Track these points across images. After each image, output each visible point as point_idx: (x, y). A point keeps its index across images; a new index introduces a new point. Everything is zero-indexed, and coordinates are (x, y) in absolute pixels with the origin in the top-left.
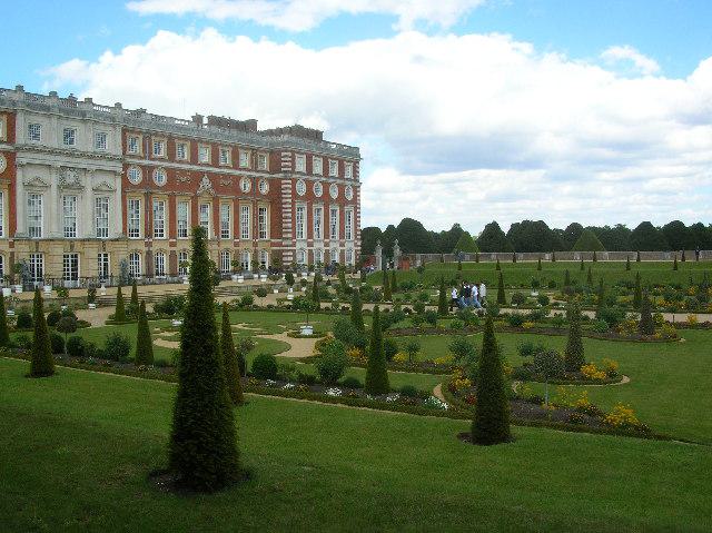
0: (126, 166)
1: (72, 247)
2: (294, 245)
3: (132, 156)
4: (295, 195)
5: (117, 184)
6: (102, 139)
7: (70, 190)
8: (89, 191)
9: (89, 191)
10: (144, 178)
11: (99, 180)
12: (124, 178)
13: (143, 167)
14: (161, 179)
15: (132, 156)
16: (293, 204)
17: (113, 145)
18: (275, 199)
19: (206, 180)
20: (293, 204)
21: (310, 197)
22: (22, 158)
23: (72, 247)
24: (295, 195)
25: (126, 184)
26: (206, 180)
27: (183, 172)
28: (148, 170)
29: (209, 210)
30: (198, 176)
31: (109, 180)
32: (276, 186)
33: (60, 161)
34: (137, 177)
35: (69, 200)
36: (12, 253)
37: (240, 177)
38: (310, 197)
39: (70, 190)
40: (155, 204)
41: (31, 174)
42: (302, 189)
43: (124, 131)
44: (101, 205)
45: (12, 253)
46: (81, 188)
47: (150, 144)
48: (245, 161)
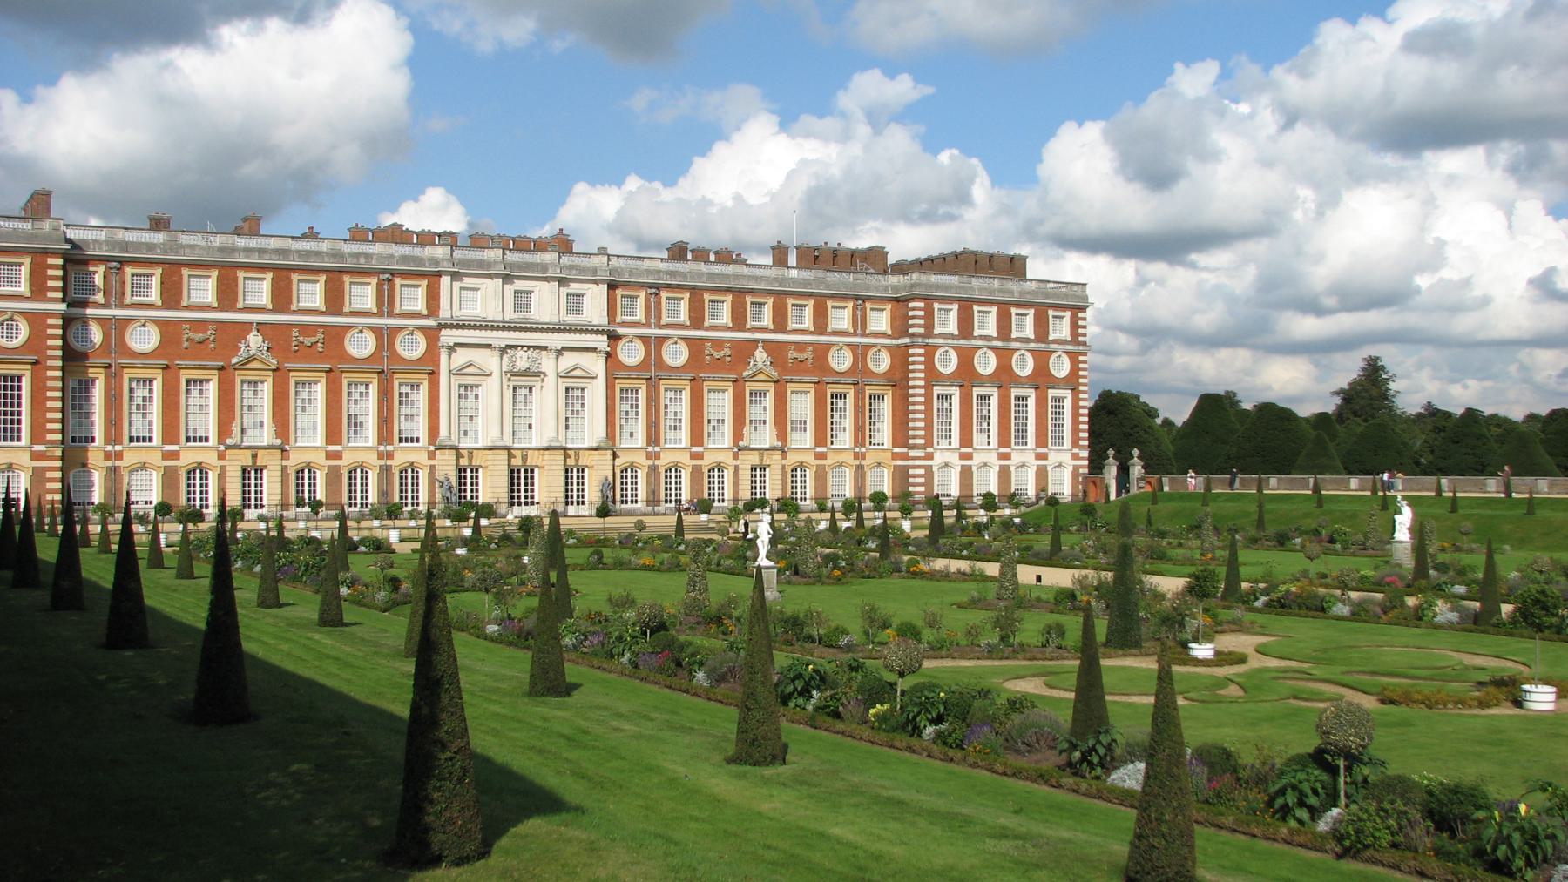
0: (614, 338)
1: (524, 458)
2: (930, 457)
3: (624, 324)
4: (933, 377)
5: (597, 365)
7: (523, 381)
8: (551, 379)
9: (551, 379)
11: (569, 360)
12: (609, 356)
13: (645, 339)
14: (676, 355)
15: (624, 324)
16: (929, 387)
18: (898, 380)
19: (760, 356)
21: (966, 376)
22: (448, 337)
23: (524, 458)
24: (933, 377)
26: (760, 356)
27: (718, 343)
28: (654, 345)
29: (769, 401)
30: (744, 351)
32: (900, 356)
33: (501, 338)
34: (632, 354)
36: (433, 467)
38: (966, 376)
39: (523, 381)
40: (665, 396)
41: (461, 357)
42: (948, 363)
43: (612, 286)
44: (572, 395)
45: (433, 467)
46: (539, 374)
47: (658, 304)
48: (841, 318)
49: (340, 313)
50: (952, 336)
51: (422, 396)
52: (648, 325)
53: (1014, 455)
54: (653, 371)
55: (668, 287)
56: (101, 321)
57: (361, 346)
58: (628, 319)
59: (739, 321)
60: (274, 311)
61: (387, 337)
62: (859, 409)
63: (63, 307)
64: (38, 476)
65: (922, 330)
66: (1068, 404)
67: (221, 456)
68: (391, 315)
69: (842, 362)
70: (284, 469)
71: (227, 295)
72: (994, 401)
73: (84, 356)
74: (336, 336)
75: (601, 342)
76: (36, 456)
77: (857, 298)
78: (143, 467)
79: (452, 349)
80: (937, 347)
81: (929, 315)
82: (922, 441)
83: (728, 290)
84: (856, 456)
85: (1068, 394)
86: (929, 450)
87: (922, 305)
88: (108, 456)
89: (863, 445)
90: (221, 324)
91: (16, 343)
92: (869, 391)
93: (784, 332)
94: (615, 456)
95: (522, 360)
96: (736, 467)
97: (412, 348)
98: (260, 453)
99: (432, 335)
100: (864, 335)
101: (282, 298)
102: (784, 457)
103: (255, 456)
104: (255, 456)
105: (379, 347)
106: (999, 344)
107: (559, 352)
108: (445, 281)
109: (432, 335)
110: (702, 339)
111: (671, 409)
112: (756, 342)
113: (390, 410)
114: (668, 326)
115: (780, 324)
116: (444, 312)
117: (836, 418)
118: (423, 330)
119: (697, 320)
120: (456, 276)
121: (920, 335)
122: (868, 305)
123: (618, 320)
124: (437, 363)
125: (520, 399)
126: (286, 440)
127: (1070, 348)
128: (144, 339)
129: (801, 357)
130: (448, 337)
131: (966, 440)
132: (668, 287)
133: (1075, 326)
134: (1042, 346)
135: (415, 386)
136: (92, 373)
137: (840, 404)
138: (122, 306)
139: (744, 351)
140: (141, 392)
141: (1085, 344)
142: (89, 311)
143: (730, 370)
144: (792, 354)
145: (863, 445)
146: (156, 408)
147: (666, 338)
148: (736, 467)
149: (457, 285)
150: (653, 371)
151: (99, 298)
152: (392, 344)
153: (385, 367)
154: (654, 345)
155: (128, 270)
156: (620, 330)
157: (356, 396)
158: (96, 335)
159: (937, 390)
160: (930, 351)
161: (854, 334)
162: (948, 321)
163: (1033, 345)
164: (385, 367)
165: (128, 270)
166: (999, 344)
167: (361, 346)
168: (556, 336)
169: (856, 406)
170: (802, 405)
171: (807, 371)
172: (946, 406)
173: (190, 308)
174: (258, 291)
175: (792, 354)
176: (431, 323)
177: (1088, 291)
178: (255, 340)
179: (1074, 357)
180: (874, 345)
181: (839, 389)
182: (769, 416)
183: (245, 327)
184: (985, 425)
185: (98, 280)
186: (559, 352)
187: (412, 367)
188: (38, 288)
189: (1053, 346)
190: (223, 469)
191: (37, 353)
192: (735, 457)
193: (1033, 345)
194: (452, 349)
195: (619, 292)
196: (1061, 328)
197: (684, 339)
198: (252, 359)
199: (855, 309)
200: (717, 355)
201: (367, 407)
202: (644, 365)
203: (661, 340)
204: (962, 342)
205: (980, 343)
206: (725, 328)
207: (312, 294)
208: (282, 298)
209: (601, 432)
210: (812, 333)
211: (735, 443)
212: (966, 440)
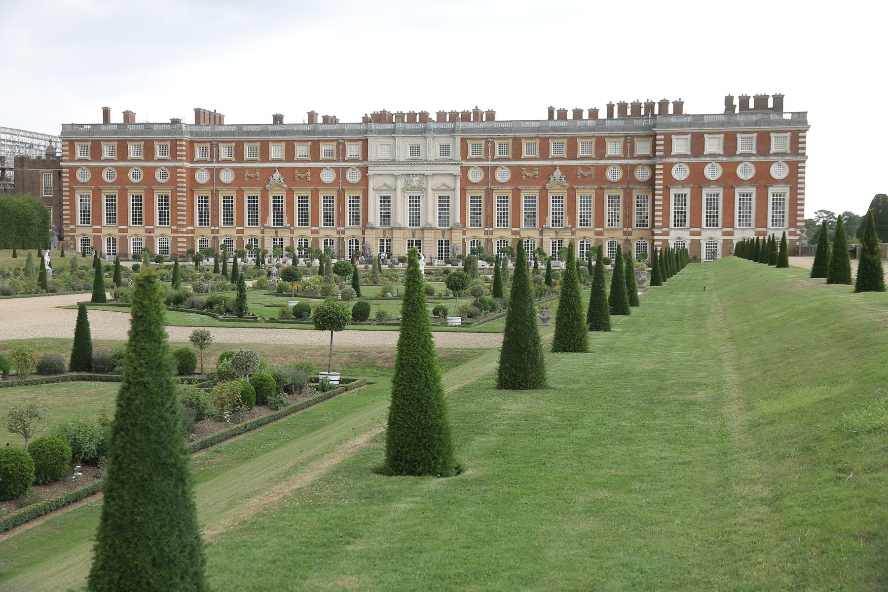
0: (465, 170)
3: (472, 160)
9: (430, 191)
10: (486, 176)
13: (485, 168)
14: (503, 176)
15: (472, 160)
16: (667, 189)
17: (456, 152)
19: (558, 174)
20: (667, 189)
22: (370, 172)
24: (670, 182)
25: (466, 183)
26: (558, 174)
27: (531, 168)
28: (489, 172)
31: (449, 181)
34: (475, 176)
37: (606, 167)
47: (493, 147)
49: (318, 161)
50: (686, 156)
52: (487, 160)
53: (736, 232)
57: (327, 177)
58: (474, 156)
60: (287, 161)
65: (662, 153)
66: (787, 197)
67: (263, 232)
68: (344, 161)
71: (265, 154)
74: (317, 172)
75: (457, 170)
76: (174, 231)
80: (672, 165)
82: (661, 224)
83: (536, 138)
84: (625, 233)
85: (785, 190)
88: (213, 232)
89: (630, 226)
90: (261, 169)
93: (575, 159)
94: (464, 233)
95: (415, 181)
96: (541, 240)
97: (353, 177)
98: (279, 231)
100: (632, 158)
101: (290, 154)
103: (277, 232)
104: (277, 232)
105: (338, 177)
106: (724, 159)
109: (365, 170)
110: (520, 167)
112: (554, 168)
113: (344, 209)
114: (499, 159)
116: (372, 156)
118: (359, 168)
121: (661, 157)
122: (635, 139)
123: (470, 155)
126: (292, 225)
127: (788, 158)
132: (499, 138)
134: (762, 159)
138: (218, 162)
143: (537, 184)
144: (581, 172)
145: (630, 226)
147: (497, 167)
154: (489, 172)
159: (673, 192)
160: (668, 167)
161: (625, 158)
162: (681, 145)
163: (753, 159)
166: (724, 159)
168: (429, 168)
169: (625, 203)
173: (248, 161)
174: (276, 151)
175: (581, 172)
177: (809, 117)
178: (277, 175)
180: (639, 165)
181: (614, 193)
183: (273, 170)
189: (771, 159)
190: (263, 238)
191: (173, 185)
192: (541, 233)
193: (753, 159)
196: (778, 143)
197: (509, 167)
199: (625, 142)
200: (531, 175)
202: (484, 182)
203: (495, 168)
204: (693, 160)
205: (708, 159)
206: (535, 159)
207: (301, 151)
208: (290, 154)
209: (458, 221)
210: (593, 159)
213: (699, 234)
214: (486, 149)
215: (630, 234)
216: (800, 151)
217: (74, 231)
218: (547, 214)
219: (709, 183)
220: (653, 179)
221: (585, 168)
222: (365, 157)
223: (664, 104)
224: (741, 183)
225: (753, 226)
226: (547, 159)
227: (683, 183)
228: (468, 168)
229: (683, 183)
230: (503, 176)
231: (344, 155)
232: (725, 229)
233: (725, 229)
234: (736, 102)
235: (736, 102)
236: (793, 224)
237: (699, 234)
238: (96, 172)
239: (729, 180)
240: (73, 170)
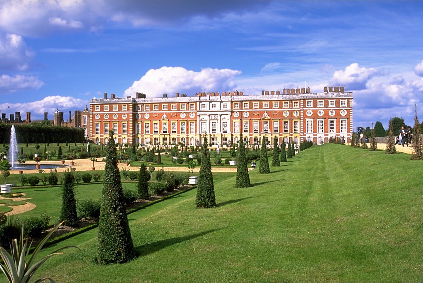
0: (232, 112)
1: (214, 136)
2: (305, 135)
4: (305, 117)
5: (228, 117)
6: (225, 106)
8: (219, 121)
10: (240, 115)
11: (223, 117)
12: (231, 116)
14: (246, 115)
17: (229, 108)
19: (266, 114)
20: (304, 119)
23: (214, 136)
24: (305, 117)
26: (266, 114)
28: (241, 113)
29: (268, 124)
30: (262, 113)
35: (214, 123)
38: (315, 116)
41: (201, 117)
42: (310, 114)
43: (232, 102)
51: (194, 125)
52: (240, 109)
54: (241, 118)
55: (245, 101)
56: (140, 114)
57: (183, 116)
58: (236, 108)
59: (261, 107)
61: (187, 114)
62: (291, 125)
63: (131, 112)
64: (128, 139)
66: (346, 122)
67: (159, 136)
69: (286, 115)
70: (170, 138)
72: (324, 122)
73: (138, 120)
75: (229, 113)
76: (128, 136)
77: (290, 100)
78: (147, 138)
79: (200, 116)
81: (305, 103)
86: (305, 133)
87: (303, 101)
88: (142, 136)
91: (287, 116)
92: (293, 121)
94: (232, 135)
96: (260, 138)
97: (192, 116)
99: (196, 113)
102: (272, 135)
106: (325, 108)
107: (221, 115)
108: (198, 103)
111: (246, 126)
115: (271, 107)
117: (286, 127)
119: (251, 108)
120: (200, 102)
121: (302, 108)
123: (234, 108)
124: (197, 118)
125: (214, 125)
128: (147, 117)
129: (275, 114)
130: (199, 113)
131: (315, 131)
132: (245, 101)
133: (348, 103)
134: (338, 108)
135: (193, 123)
136: (139, 122)
137: (287, 124)
139: (262, 113)
140: (147, 125)
141: (351, 107)
142: (138, 112)
143: (259, 118)
146: (149, 128)
147: (244, 111)
148: (260, 138)
149: (201, 104)
150: (241, 118)
151: (140, 110)
152: (189, 115)
153: (187, 119)
154: (241, 113)
155: (145, 105)
156: (233, 110)
157: (183, 125)
158: (140, 116)
160: (305, 112)
161: (290, 108)
164: (187, 119)
165: (145, 105)
166: (325, 108)
167: (183, 116)
170: (277, 125)
171: (277, 117)
172: (310, 123)
176: (195, 111)
179: (348, 111)
182: (268, 127)
184: (321, 128)
185: (140, 108)
186: (221, 115)
187: (193, 119)
188: (128, 109)
194: (200, 116)
195: (234, 103)
197: (248, 111)
198: (164, 119)
201: (184, 127)
211: (260, 132)
212: (315, 131)
213: (316, 135)
214: (240, 105)
215: (292, 135)
216: (350, 106)
217: (94, 136)
218: (262, 128)
219: (319, 117)
220: (300, 115)
221: (275, 112)
222: (196, 109)
223: (303, 89)
224: (331, 117)
225: (335, 132)
226: (262, 109)
227: (310, 117)
228: (233, 112)
229: (310, 117)
230: (246, 115)
231: (189, 108)
232: (326, 133)
233: (326, 133)
234: (328, 89)
235: (328, 89)
236: (348, 132)
237: (316, 135)
238: (102, 116)
239: (326, 116)
240: (94, 115)
